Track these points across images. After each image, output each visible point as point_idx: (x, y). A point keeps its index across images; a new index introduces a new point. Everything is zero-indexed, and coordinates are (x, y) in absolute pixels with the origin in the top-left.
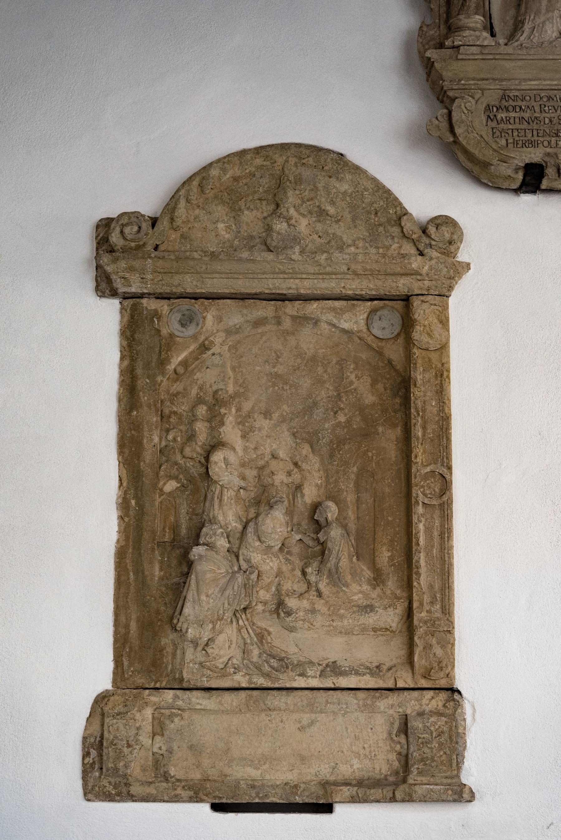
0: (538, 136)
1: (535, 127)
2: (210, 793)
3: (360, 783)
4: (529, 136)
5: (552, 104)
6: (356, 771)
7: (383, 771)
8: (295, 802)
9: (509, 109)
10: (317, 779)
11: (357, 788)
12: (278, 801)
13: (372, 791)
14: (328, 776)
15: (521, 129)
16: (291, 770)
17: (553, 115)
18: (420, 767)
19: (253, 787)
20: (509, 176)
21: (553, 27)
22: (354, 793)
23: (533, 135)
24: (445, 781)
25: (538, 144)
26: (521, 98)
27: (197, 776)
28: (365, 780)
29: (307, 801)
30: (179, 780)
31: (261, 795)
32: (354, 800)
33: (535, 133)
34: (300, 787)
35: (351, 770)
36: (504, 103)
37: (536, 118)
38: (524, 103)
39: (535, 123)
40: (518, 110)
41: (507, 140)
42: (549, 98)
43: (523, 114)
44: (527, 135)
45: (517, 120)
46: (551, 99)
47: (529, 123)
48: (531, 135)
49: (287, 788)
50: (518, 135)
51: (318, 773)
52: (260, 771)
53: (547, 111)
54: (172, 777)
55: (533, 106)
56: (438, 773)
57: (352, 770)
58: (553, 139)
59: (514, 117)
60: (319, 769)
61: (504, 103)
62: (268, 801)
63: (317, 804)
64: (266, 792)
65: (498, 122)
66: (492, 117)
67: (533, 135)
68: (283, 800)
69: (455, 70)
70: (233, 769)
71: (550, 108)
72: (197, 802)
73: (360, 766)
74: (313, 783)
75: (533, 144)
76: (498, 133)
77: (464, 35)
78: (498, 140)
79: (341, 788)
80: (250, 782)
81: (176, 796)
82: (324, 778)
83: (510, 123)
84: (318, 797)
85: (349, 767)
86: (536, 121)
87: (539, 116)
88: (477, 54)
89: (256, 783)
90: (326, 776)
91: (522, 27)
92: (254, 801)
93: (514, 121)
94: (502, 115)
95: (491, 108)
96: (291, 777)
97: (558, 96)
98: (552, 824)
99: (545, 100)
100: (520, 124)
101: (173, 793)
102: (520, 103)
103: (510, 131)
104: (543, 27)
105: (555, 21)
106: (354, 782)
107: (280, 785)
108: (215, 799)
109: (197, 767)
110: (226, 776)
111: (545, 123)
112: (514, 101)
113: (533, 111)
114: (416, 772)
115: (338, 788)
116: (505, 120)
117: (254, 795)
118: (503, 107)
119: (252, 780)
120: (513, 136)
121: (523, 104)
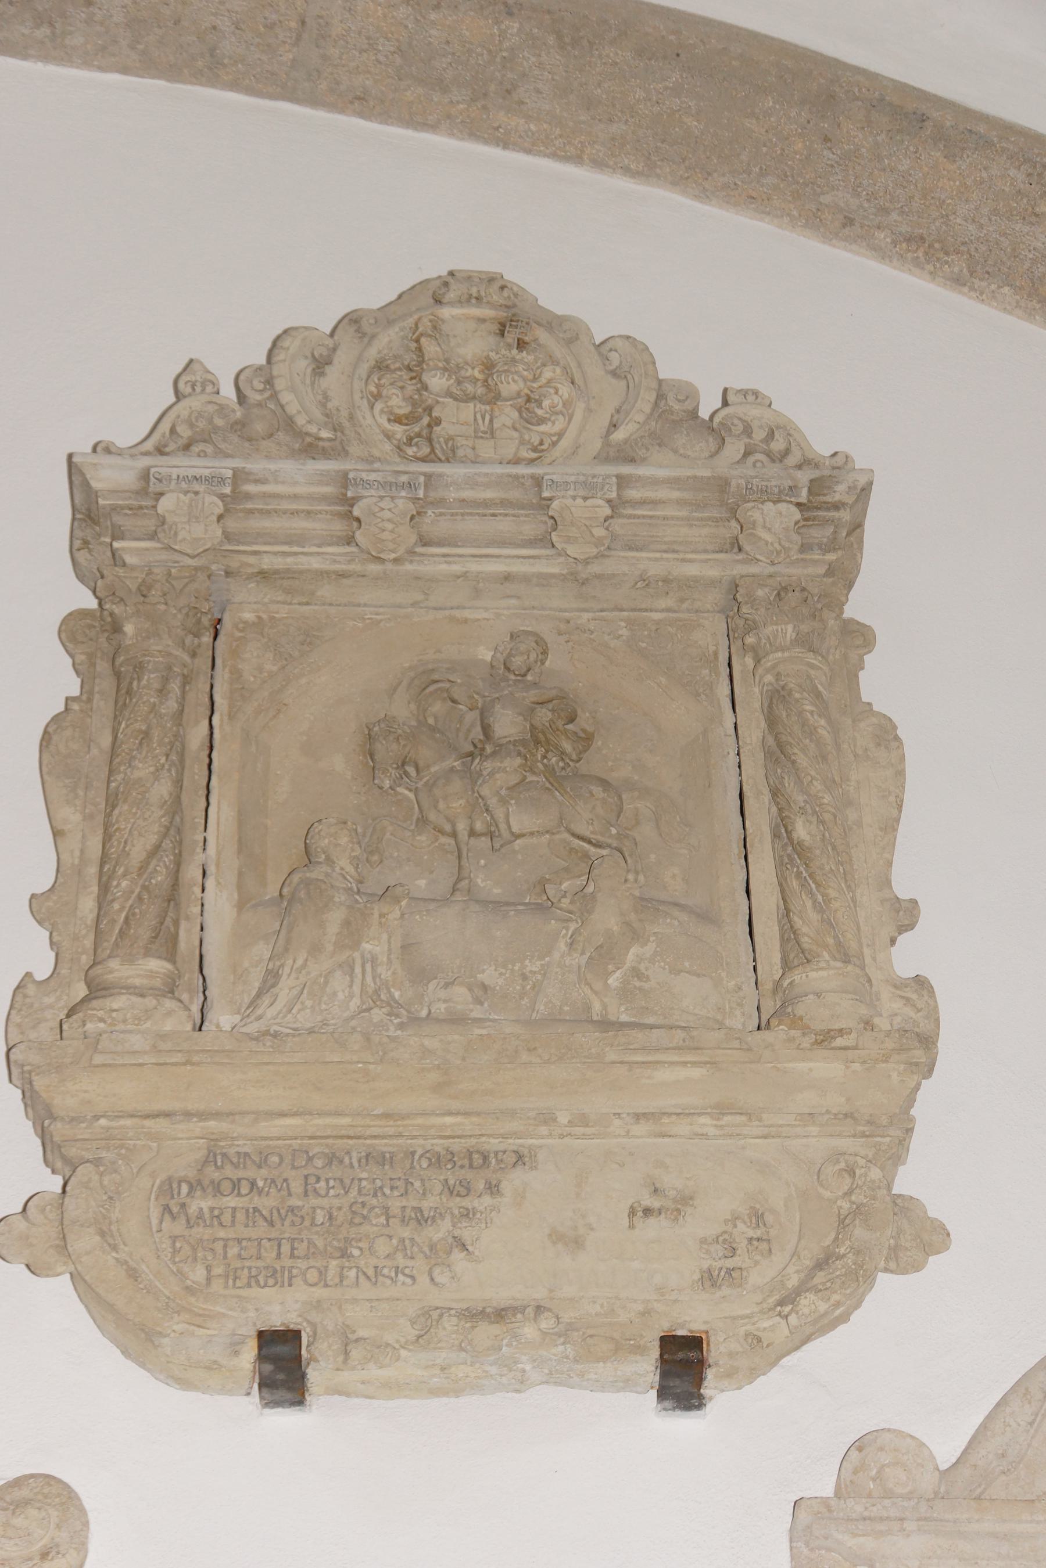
0: (292, 1256)
1: (289, 1232)
4: (269, 1255)
5: (338, 1174)
9: (222, 1188)
15: (249, 1239)
17: (336, 1202)
20: (215, 1362)
21: (351, 986)
23: (279, 1254)
25: (290, 1279)
26: (257, 1159)
33: (286, 1248)
36: (212, 1173)
37: (292, 1210)
38: (264, 1172)
39: (287, 1223)
40: (244, 1191)
41: (209, 1269)
42: (332, 1159)
43: (257, 1201)
44: (264, 1254)
45: (240, 1216)
46: (335, 1163)
47: (271, 1224)
48: (274, 1254)
50: (239, 1255)
53: (323, 1192)
55: (285, 1180)
58: (334, 1263)
59: (234, 1209)
61: (212, 1173)
65: (188, 1221)
66: (175, 1210)
67: (279, 1254)
69: (86, 1092)
71: (332, 1183)
75: (277, 1277)
76: (187, 1250)
77: (115, 1006)
78: (186, 1268)
83: (221, 1224)
86: (290, 1217)
87: (300, 1203)
88: (145, 1053)
91: (273, 986)
93: (234, 1217)
94: (201, 1204)
95: (175, 1186)
97: (354, 1155)
99: (319, 1163)
100: (247, 1226)
102: (251, 1173)
103: (219, 1246)
104: (326, 982)
105: (358, 970)
111: (313, 1224)
112: (236, 1166)
113: (285, 1193)
116: (207, 1216)
118: (206, 1182)
120: (225, 1257)
121: (260, 1177)
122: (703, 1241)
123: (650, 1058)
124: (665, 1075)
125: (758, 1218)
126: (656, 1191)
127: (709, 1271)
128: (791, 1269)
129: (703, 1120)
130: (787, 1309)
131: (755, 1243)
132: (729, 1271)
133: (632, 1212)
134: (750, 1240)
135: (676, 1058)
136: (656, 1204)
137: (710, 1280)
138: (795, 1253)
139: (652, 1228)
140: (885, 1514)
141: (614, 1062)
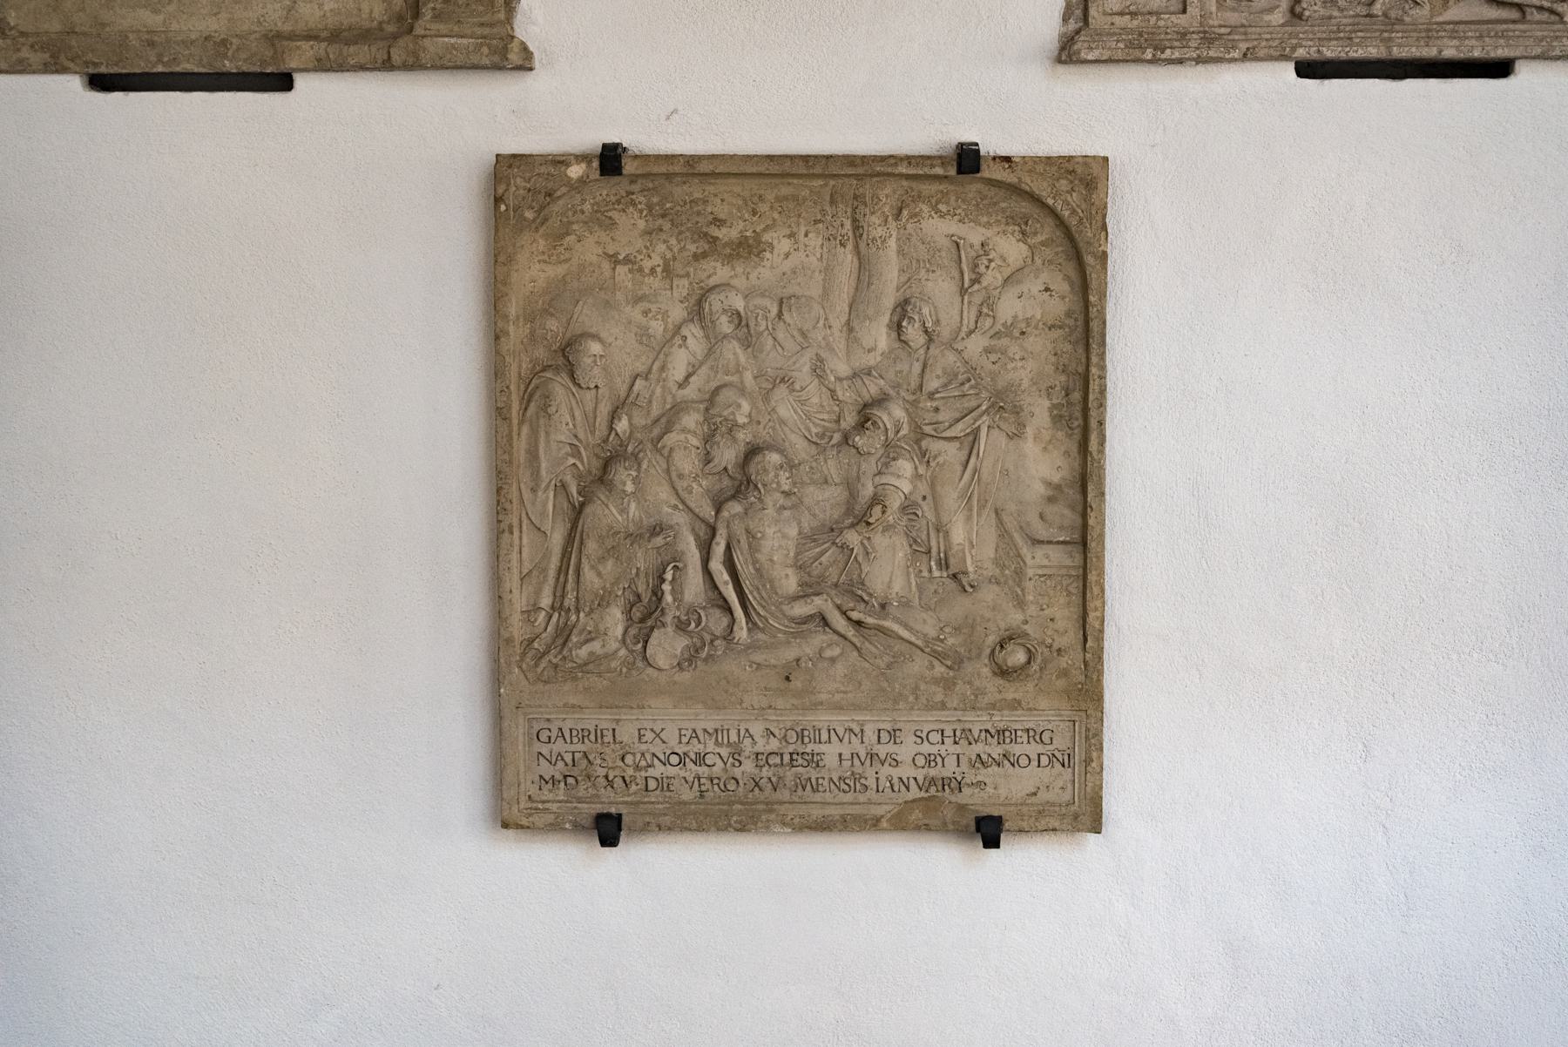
2: (78, 57)
3: (335, 36)
6: (328, 14)
7: (376, 14)
8: (224, 70)
10: (262, 28)
11: (326, 44)
12: (196, 70)
13: (352, 49)
14: (279, 24)
16: (215, 15)
18: (438, 6)
19: (151, 44)
22: (322, 52)
24: (479, 31)
27: (54, 26)
28: (344, 30)
29: (246, 68)
30: (23, 34)
31: (166, 59)
32: (323, 66)
34: (231, 44)
35: (318, 13)
49: (210, 45)
51: (262, 19)
52: (161, 17)
54: (11, 29)
56: (469, 17)
57: (322, 13)
60: (265, 11)
62: (178, 69)
63: (262, 74)
64: (174, 54)
68: (204, 67)
70: (115, 12)
72: (57, 72)
73: (336, 6)
74: (254, 36)
79: (299, 43)
80: (146, 37)
81: (21, 61)
82: (273, 27)
84: (263, 62)
85: (316, 7)
89: (156, 38)
90: (276, 24)
92: (155, 70)
96: (215, 26)
98: (675, 111)
101: (14, 58)
106: (324, 34)
107: (197, 39)
108: (88, 67)
109: (54, 10)
110: (103, 25)
114: (429, 17)
115: (295, 44)
117: (153, 59)
119: (148, 32)
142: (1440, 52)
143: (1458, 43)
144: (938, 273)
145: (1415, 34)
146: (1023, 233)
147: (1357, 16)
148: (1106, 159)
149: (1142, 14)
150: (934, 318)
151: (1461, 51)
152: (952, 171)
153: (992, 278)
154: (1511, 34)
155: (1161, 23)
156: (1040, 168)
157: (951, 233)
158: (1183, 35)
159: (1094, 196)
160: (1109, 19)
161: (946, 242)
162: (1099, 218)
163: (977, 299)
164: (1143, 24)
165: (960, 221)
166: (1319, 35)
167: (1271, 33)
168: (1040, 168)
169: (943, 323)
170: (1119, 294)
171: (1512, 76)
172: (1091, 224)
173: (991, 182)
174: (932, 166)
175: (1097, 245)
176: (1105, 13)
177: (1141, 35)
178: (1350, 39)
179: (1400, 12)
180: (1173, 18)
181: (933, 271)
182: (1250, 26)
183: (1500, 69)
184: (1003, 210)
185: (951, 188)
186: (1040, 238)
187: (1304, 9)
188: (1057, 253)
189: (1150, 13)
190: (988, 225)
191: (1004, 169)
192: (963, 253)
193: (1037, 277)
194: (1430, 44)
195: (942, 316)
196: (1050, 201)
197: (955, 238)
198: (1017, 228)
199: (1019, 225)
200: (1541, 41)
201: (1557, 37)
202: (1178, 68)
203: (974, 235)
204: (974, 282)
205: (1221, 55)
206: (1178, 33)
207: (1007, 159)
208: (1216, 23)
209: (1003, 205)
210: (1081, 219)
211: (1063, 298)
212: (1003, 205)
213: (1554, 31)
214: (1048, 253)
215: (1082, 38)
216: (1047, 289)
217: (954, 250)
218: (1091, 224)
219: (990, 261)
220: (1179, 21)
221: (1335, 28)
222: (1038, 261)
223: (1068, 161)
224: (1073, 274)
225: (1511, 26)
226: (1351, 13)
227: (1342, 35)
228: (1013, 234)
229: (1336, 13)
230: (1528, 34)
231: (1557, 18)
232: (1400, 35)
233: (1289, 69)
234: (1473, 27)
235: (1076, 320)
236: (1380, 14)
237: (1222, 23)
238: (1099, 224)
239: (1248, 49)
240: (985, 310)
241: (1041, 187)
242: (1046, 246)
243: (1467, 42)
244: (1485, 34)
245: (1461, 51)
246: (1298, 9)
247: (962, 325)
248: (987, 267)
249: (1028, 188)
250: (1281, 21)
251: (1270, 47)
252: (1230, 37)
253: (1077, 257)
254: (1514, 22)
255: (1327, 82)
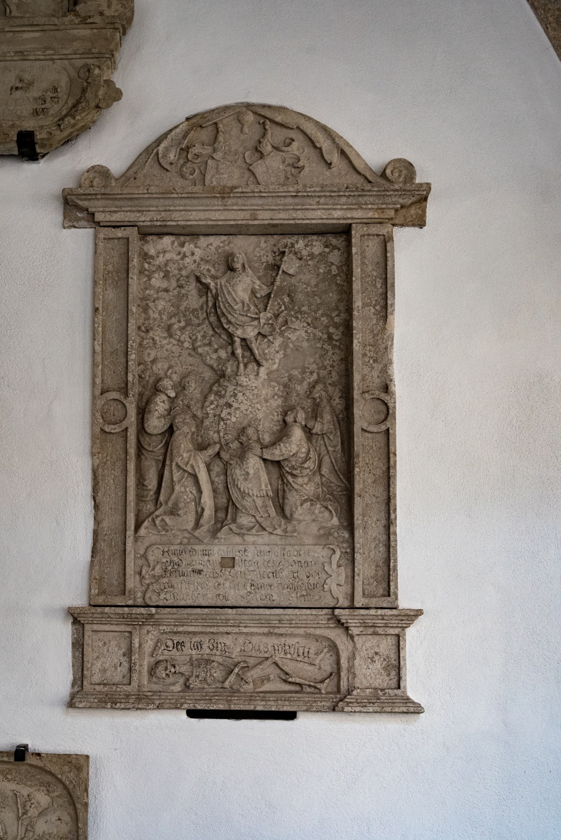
122: (35, 99)
123: (21, 29)
124: (26, 36)
125: (55, 89)
126: (21, 80)
127: (36, 109)
128: (64, 108)
129: (39, 53)
130: (61, 122)
131: (53, 99)
132: (43, 109)
133: (12, 89)
134: (51, 98)
135: (30, 29)
136: (19, 85)
137: (36, 113)
138: (66, 102)
139: (18, 94)
140: (90, 193)
141: (8, 32)
142: (255, 707)
143: (265, 704)
144: (7, 808)
145: (244, 698)
146: (48, 791)
147: (217, 688)
148: (87, 757)
149: (110, 685)
150: (4, 831)
151: (266, 708)
152: (12, 759)
153: (33, 812)
154: (292, 699)
155: (118, 690)
156: (55, 760)
157: (13, 789)
158: (128, 696)
159: (81, 775)
160: (93, 686)
161: (11, 794)
162: (83, 785)
163: (25, 823)
164: (110, 690)
165: (17, 784)
166: (196, 697)
167: (172, 696)
168: (55, 760)
169: (9, 833)
170: (99, 821)
171: (295, 720)
172: (79, 788)
173: (31, 765)
174: (3, 757)
175: (82, 799)
176: (91, 684)
177: (107, 696)
178: (211, 700)
179: (238, 687)
180: (124, 687)
181: (4, 808)
182: (163, 692)
183: (291, 716)
184: (38, 780)
185: (13, 767)
186: (56, 794)
187: (191, 684)
188: (64, 802)
189: (114, 684)
190: (31, 786)
191: (37, 760)
192: (18, 799)
193: (54, 813)
194: (251, 703)
195: (9, 830)
196: (59, 776)
197: (15, 792)
198: (45, 788)
199: (46, 787)
200: (307, 703)
201: (315, 701)
202: (128, 711)
203: (25, 791)
204: (25, 813)
205: (145, 707)
206: (125, 695)
207: (39, 755)
208: (147, 690)
209: (38, 777)
210: (74, 786)
211: (67, 824)
212: (38, 777)
213: (314, 698)
214: (60, 801)
215: (78, 696)
216: (59, 819)
217: (14, 798)
218: (79, 788)
219: (32, 804)
220: (127, 689)
221: (205, 694)
222: (55, 805)
223: (69, 757)
224: (72, 812)
225: (293, 695)
226: (214, 686)
227: (207, 698)
228: (43, 791)
229: (206, 686)
230: (301, 699)
231: (318, 691)
232: (236, 698)
233: (183, 715)
234: (274, 695)
235: (73, 835)
236: (228, 687)
237: (150, 690)
238: (84, 788)
239: (159, 704)
240: (29, 828)
241: (55, 769)
242: (59, 798)
243: (269, 703)
244: (279, 699)
245: (266, 708)
246: (188, 684)
247: (18, 835)
248: (30, 807)
249: (49, 770)
250: (180, 689)
251: (171, 703)
252: (152, 697)
253: (73, 802)
254: (296, 692)
255: (202, 720)
